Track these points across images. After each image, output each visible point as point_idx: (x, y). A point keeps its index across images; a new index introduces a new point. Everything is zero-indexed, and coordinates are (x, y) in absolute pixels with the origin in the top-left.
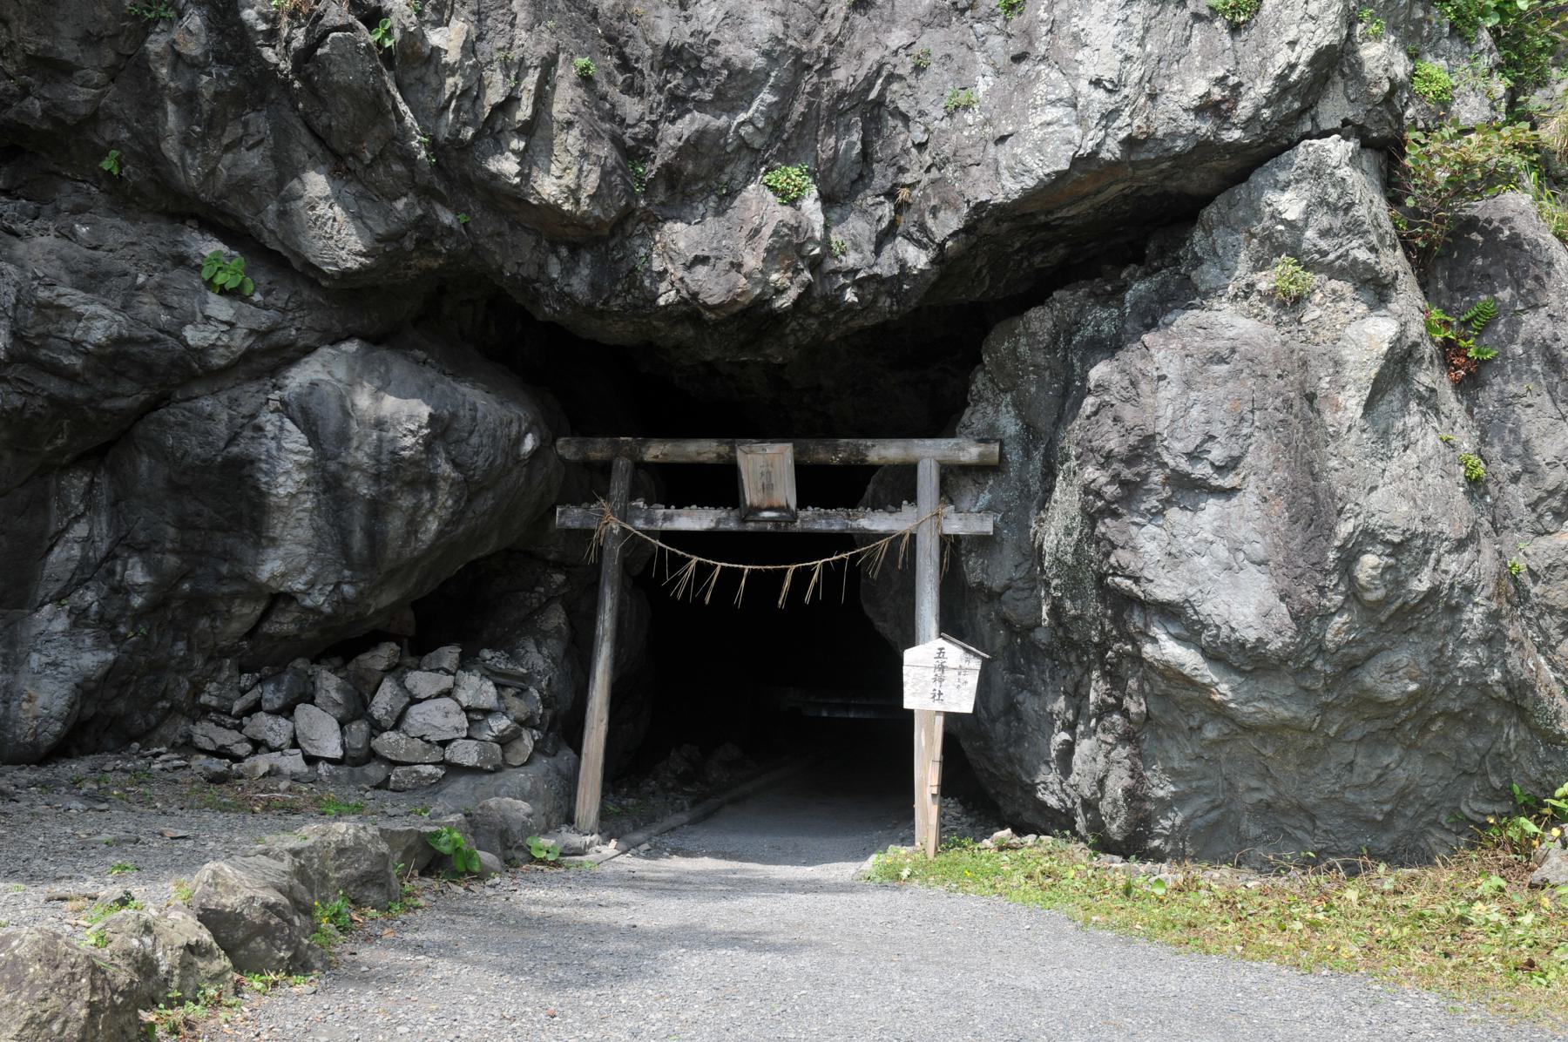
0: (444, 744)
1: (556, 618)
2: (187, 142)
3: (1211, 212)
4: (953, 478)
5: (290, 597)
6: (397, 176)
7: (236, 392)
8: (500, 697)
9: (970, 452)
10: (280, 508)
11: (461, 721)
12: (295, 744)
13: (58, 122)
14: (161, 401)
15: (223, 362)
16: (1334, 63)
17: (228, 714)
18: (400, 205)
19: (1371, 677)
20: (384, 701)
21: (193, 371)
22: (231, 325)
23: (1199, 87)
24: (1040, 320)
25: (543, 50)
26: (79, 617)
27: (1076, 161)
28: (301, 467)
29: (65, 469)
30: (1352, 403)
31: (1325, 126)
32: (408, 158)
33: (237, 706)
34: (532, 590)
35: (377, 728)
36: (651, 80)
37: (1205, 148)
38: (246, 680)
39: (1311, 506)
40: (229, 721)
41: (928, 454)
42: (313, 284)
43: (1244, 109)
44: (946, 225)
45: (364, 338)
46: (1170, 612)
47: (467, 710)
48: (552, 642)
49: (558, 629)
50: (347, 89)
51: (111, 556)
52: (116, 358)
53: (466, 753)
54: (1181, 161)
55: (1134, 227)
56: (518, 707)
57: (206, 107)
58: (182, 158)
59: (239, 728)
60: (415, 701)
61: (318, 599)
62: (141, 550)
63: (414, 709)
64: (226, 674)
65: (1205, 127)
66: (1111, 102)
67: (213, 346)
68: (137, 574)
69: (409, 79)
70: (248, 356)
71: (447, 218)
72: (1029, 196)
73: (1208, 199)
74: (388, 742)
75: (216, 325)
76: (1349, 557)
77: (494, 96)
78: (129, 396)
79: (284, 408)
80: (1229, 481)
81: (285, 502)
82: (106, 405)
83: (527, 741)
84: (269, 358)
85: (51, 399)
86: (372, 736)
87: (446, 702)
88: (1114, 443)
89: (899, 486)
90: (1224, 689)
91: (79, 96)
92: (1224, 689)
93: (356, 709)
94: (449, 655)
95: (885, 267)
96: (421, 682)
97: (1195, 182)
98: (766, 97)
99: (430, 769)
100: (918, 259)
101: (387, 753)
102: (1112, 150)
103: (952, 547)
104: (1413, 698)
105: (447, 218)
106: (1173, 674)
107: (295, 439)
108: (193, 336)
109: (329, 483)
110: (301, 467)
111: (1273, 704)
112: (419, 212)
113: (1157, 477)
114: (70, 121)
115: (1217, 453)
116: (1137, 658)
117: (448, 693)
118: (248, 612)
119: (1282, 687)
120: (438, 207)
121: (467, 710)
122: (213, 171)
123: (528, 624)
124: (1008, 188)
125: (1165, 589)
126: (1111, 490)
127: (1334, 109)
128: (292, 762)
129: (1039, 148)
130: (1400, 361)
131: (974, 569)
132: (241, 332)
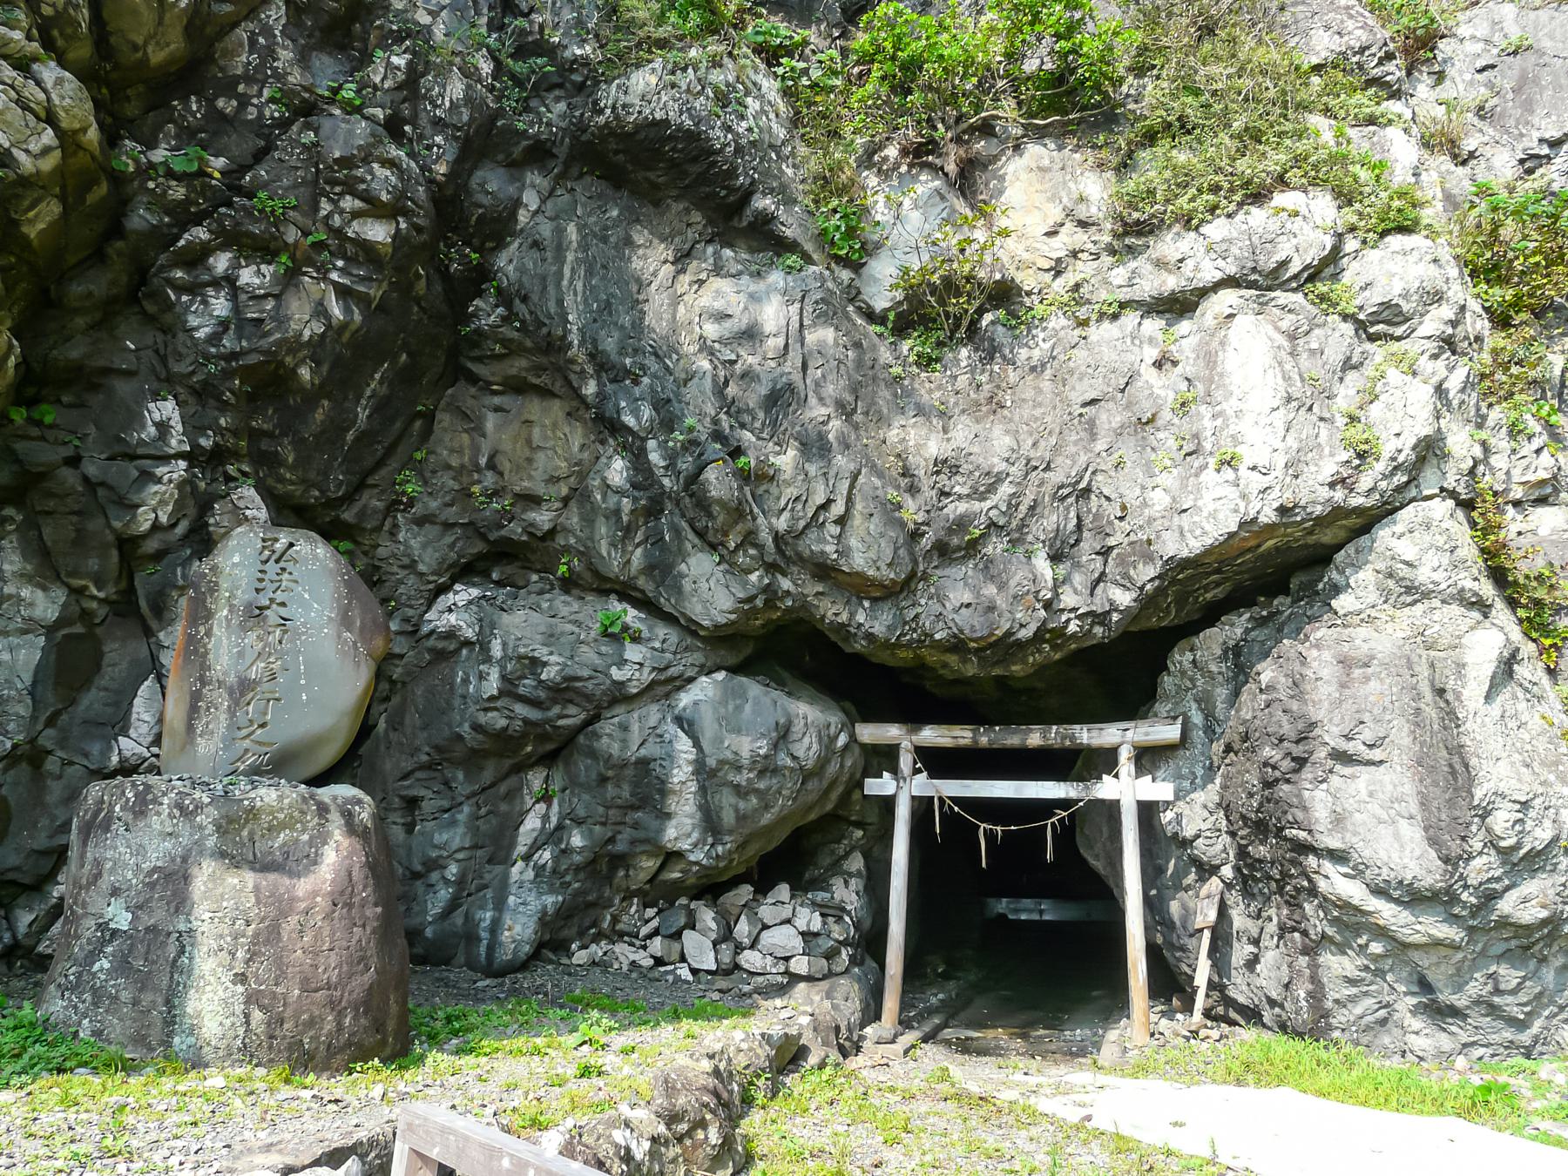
0: (787, 959)
1: (856, 863)
2: (613, 545)
3: (1340, 557)
5: (679, 855)
6: (752, 557)
7: (644, 711)
8: (824, 923)
10: (674, 792)
11: (798, 943)
12: (683, 959)
13: (531, 534)
14: (595, 718)
15: (635, 691)
16: (1430, 450)
17: (637, 937)
18: (754, 577)
19: (1506, 905)
20: (743, 929)
21: (619, 696)
22: (641, 664)
25: (852, 466)
26: (539, 870)
27: (1242, 525)
28: (690, 763)
29: (531, 766)
31: (1426, 492)
32: (760, 547)
33: (644, 931)
34: (839, 842)
35: (739, 948)
36: (925, 483)
37: (1338, 513)
38: (650, 912)
39: (1449, 773)
40: (638, 943)
42: (694, 634)
43: (1365, 482)
44: (1146, 573)
45: (728, 669)
47: (802, 934)
48: (853, 881)
49: (859, 871)
50: (720, 502)
51: (560, 827)
52: (564, 691)
53: (800, 965)
54: (1320, 521)
56: (837, 933)
57: (625, 519)
58: (609, 554)
59: (645, 948)
60: (765, 927)
61: (698, 856)
62: (579, 822)
63: (765, 934)
64: (633, 910)
65: (1339, 495)
66: (1265, 481)
67: (630, 680)
68: (577, 840)
69: (760, 491)
70: (652, 685)
71: (786, 584)
72: (1209, 551)
73: (1339, 547)
74: (750, 959)
75: (634, 665)
77: (820, 499)
78: (573, 716)
79: (679, 720)
80: (1376, 754)
81: (677, 788)
82: (561, 722)
83: (845, 954)
84: (665, 686)
85: (526, 721)
86: (737, 954)
87: (786, 929)
88: (1287, 729)
89: (1104, 761)
90: (1387, 913)
91: (543, 518)
92: (1387, 913)
93: (726, 934)
94: (783, 891)
95: (1099, 606)
96: (766, 912)
97: (1327, 537)
98: (1005, 489)
99: (779, 979)
100: (1124, 598)
101: (746, 966)
102: (1268, 516)
104: (1544, 922)
105: (786, 584)
107: (684, 744)
108: (616, 674)
109: (705, 774)
110: (690, 763)
112: (766, 581)
113: (1321, 753)
114: (539, 534)
115: (1368, 735)
116: (1313, 892)
117: (788, 921)
118: (649, 864)
120: (779, 577)
121: (802, 934)
122: (629, 561)
123: (836, 868)
124: (1193, 546)
126: (1286, 764)
128: (684, 973)
129: (1213, 515)
132: (646, 670)
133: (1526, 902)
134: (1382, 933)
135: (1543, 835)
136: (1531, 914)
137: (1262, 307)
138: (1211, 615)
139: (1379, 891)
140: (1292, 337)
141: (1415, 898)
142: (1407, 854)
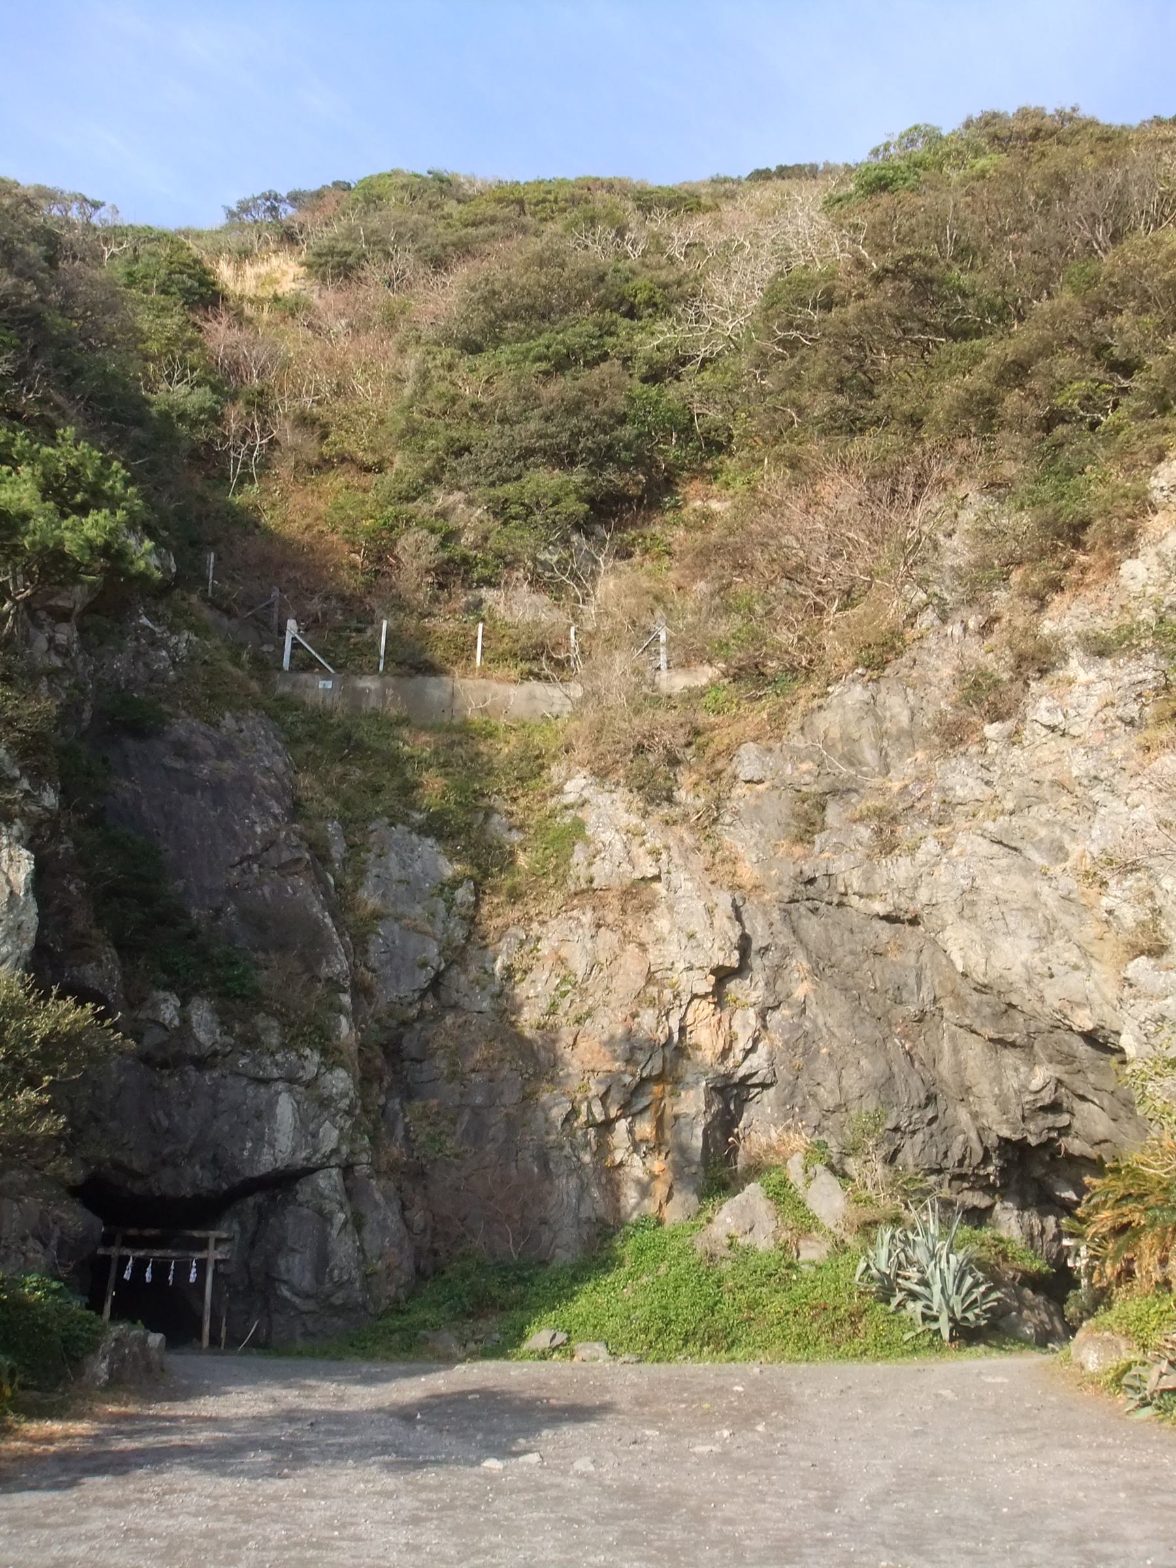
4: (219, 1241)
9: (225, 1235)
16: (335, 1151)
19: (333, 1299)
23: (304, 1155)
24: (251, 1201)
30: (334, 1233)
39: (323, 1259)
41: (213, 1234)
44: (237, 1180)
46: (285, 1282)
55: (284, 1182)
76: (332, 1270)
89: (202, 1245)
90: (297, 1300)
92: (297, 1300)
100: (225, 1186)
103: (217, 1262)
106: (286, 1299)
111: (309, 1305)
119: (312, 1302)
124: (256, 1174)
125: (285, 1277)
127: (333, 1162)
130: (345, 1224)
131: (221, 1267)
133: (338, 1299)
134: (295, 1307)
135: (345, 1278)
136: (340, 1302)
137: (290, 1091)
138: (249, 1193)
139: (297, 1295)
140: (298, 1103)
141: (307, 1296)
142: (306, 1281)
